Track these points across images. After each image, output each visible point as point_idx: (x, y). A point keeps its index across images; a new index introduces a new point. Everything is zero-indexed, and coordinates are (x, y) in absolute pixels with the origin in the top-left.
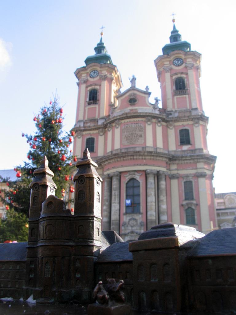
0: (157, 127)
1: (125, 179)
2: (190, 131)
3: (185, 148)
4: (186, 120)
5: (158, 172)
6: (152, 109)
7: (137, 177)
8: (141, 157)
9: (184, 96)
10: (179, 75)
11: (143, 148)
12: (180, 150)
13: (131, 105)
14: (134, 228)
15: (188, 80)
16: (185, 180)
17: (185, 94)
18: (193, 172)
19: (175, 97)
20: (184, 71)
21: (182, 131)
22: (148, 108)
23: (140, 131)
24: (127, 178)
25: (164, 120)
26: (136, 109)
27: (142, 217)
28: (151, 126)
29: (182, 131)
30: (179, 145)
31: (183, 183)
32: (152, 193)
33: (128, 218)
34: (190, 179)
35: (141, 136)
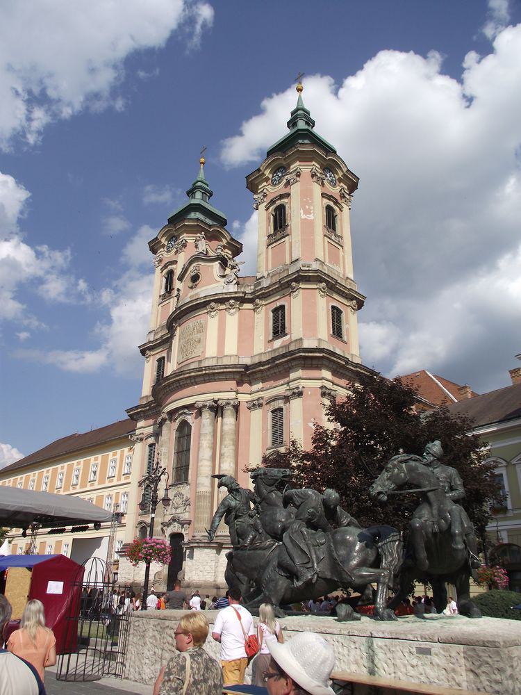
0: (229, 318)
1: (176, 425)
2: (286, 308)
3: (278, 343)
4: (280, 289)
5: (216, 402)
6: (224, 284)
7: (190, 419)
8: (189, 381)
9: (283, 240)
10: (278, 203)
11: (200, 361)
12: (269, 350)
13: (192, 288)
14: (179, 511)
15: (290, 208)
16: (272, 408)
17: (284, 237)
18: (281, 390)
19: (270, 247)
20: (286, 191)
21: (275, 311)
22: (219, 284)
23: (199, 332)
24: (177, 422)
25: (242, 300)
26: (197, 294)
27: (190, 488)
28: (217, 318)
29: (275, 311)
30: (270, 341)
31: (270, 415)
32: (206, 442)
33: (174, 493)
34: (280, 404)
35: (199, 341)
